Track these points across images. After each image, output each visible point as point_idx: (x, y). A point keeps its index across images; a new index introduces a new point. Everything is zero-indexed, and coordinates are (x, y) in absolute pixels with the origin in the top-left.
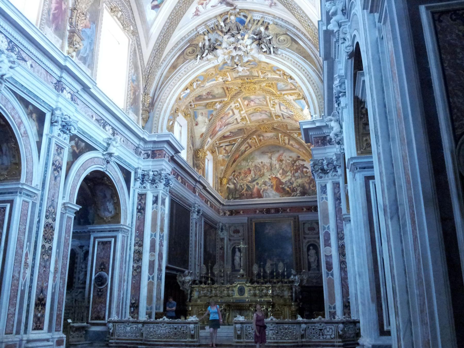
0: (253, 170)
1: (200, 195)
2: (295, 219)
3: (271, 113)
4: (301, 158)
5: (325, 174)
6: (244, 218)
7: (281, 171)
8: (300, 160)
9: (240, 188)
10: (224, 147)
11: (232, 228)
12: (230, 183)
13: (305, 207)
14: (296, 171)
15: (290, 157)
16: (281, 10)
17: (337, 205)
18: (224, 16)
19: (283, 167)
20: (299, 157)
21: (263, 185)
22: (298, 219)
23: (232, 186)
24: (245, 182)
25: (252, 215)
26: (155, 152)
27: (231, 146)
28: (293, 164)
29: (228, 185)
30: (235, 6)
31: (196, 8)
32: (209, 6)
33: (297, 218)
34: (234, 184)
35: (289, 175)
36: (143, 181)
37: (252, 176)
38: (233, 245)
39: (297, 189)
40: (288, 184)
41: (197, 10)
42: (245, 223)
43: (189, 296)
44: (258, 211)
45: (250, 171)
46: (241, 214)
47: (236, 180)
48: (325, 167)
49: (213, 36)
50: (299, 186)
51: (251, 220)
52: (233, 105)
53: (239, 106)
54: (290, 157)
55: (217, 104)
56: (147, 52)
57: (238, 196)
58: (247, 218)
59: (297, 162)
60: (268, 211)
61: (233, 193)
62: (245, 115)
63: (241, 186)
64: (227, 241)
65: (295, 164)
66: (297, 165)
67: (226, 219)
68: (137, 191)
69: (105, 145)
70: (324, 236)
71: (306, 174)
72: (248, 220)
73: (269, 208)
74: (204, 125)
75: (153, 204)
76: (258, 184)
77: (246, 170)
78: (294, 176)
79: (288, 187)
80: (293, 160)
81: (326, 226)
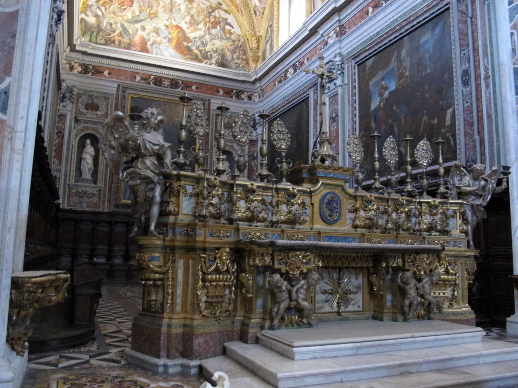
4: (224, 6)
7: (188, 19)
8: (221, 9)
9: (109, 27)
11: (84, 99)
12: (88, 13)
13: (222, 88)
14: (214, 27)
19: (193, 11)
20: (220, 4)
21: (154, 34)
23: (91, 20)
24: (120, 18)
25: (128, 82)
28: (210, 13)
29: (83, 16)
33: (206, 103)
34: (97, 16)
35: (201, 29)
37: (134, 12)
38: (82, 130)
39: (211, 55)
40: (199, 43)
42: (113, 94)
43: (155, 210)
44: (138, 78)
46: (105, 76)
50: (216, 52)
51: (124, 92)
57: (103, 42)
58: (116, 85)
59: (216, 11)
60: (158, 81)
61: (92, 32)
63: (111, 25)
64: (71, 123)
65: (213, 14)
66: (215, 17)
67: (74, 78)
71: (228, 36)
73: (159, 77)
76: (143, 28)
78: (210, 34)
79: (197, 48)
80: (211, 7)
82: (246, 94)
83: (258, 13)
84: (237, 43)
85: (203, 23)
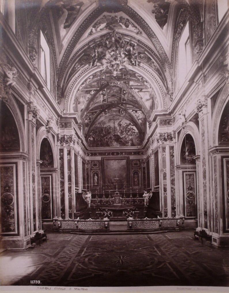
0: (104, 130)
1: (80, 145)
2: (127, 158)
3: (120, 98)
5: (165, 141)
6: (99, 157)
7: (120, 131)
10: (88, 116)
12: (91, 137)
14: (129, 132)
15: (125, 123)
16: (144, 37)
17: (171, 159)
18: (107, 36)
19: (121, 129)
21: (110, 139)
22: (129, 158)
26: (67, 124)
27: (93, 116)
30: (114, 30)
31: (91, 30)
32: (98, 29)
33: (128, 158)
34: (93, 138)
35: (124, 134)
36: (61, 141)
37: (103, 133)
39: (129, 142)
41: (92, 31)
42: (100, 160)
45: (103, 130)
46: (97, 155)
47: (94, 135)
48: (166, 137)
49: (100, 50)
52: (101, 92)
53: (105, 93)
54: (125, 123)
55: (93, 91)
56: (60, 58)
58: (101, 157)
62: (106, 98)
65: (128, 128)
66: (129, 128)
68: (59, 147)
69: (47, 122)
70: (163, 175)
71: (134, 134)
72: (101, 159)
74: (84, 104)
75: (68, 155)
77: (100, 129)
78: (127, 135)
80: (127, 125)
81: (165, 170)
82: (141, 152)
83: (142, 125)
84: (137, 135)
85: (125, 132)
